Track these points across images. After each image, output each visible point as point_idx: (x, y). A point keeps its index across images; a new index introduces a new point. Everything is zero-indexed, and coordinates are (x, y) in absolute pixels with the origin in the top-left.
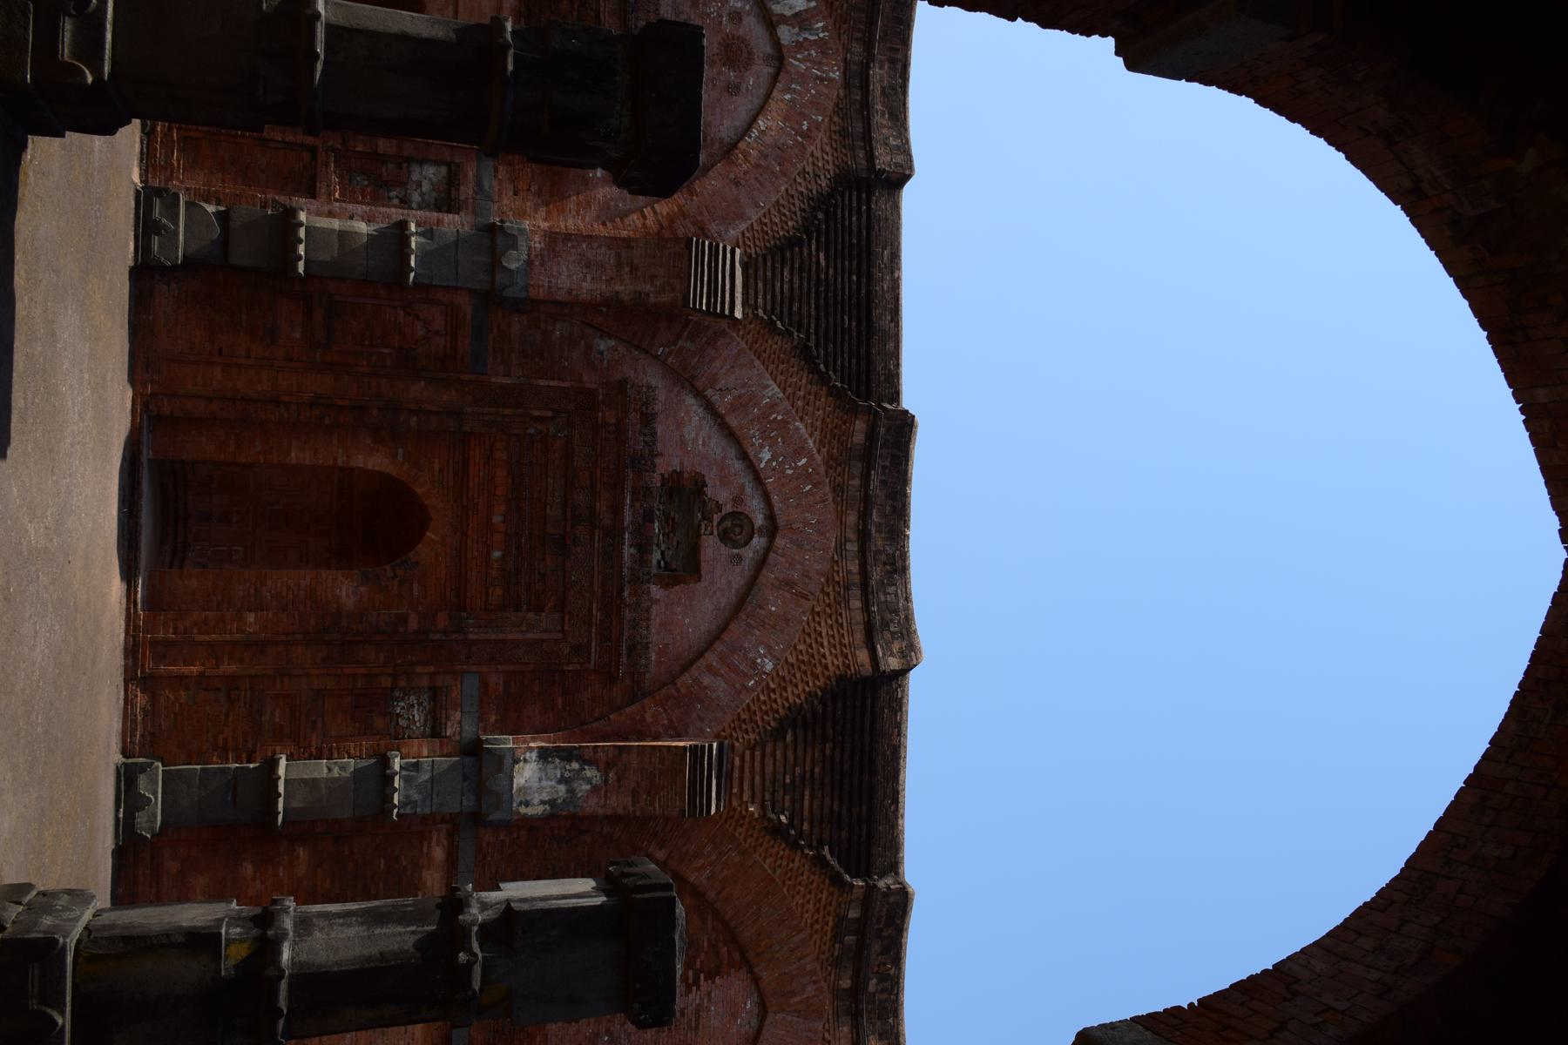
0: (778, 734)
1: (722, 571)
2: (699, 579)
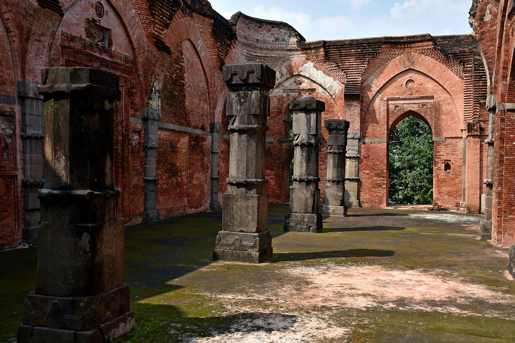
0: (153, 15)
1: (109, 21)
2: (110, 30)
